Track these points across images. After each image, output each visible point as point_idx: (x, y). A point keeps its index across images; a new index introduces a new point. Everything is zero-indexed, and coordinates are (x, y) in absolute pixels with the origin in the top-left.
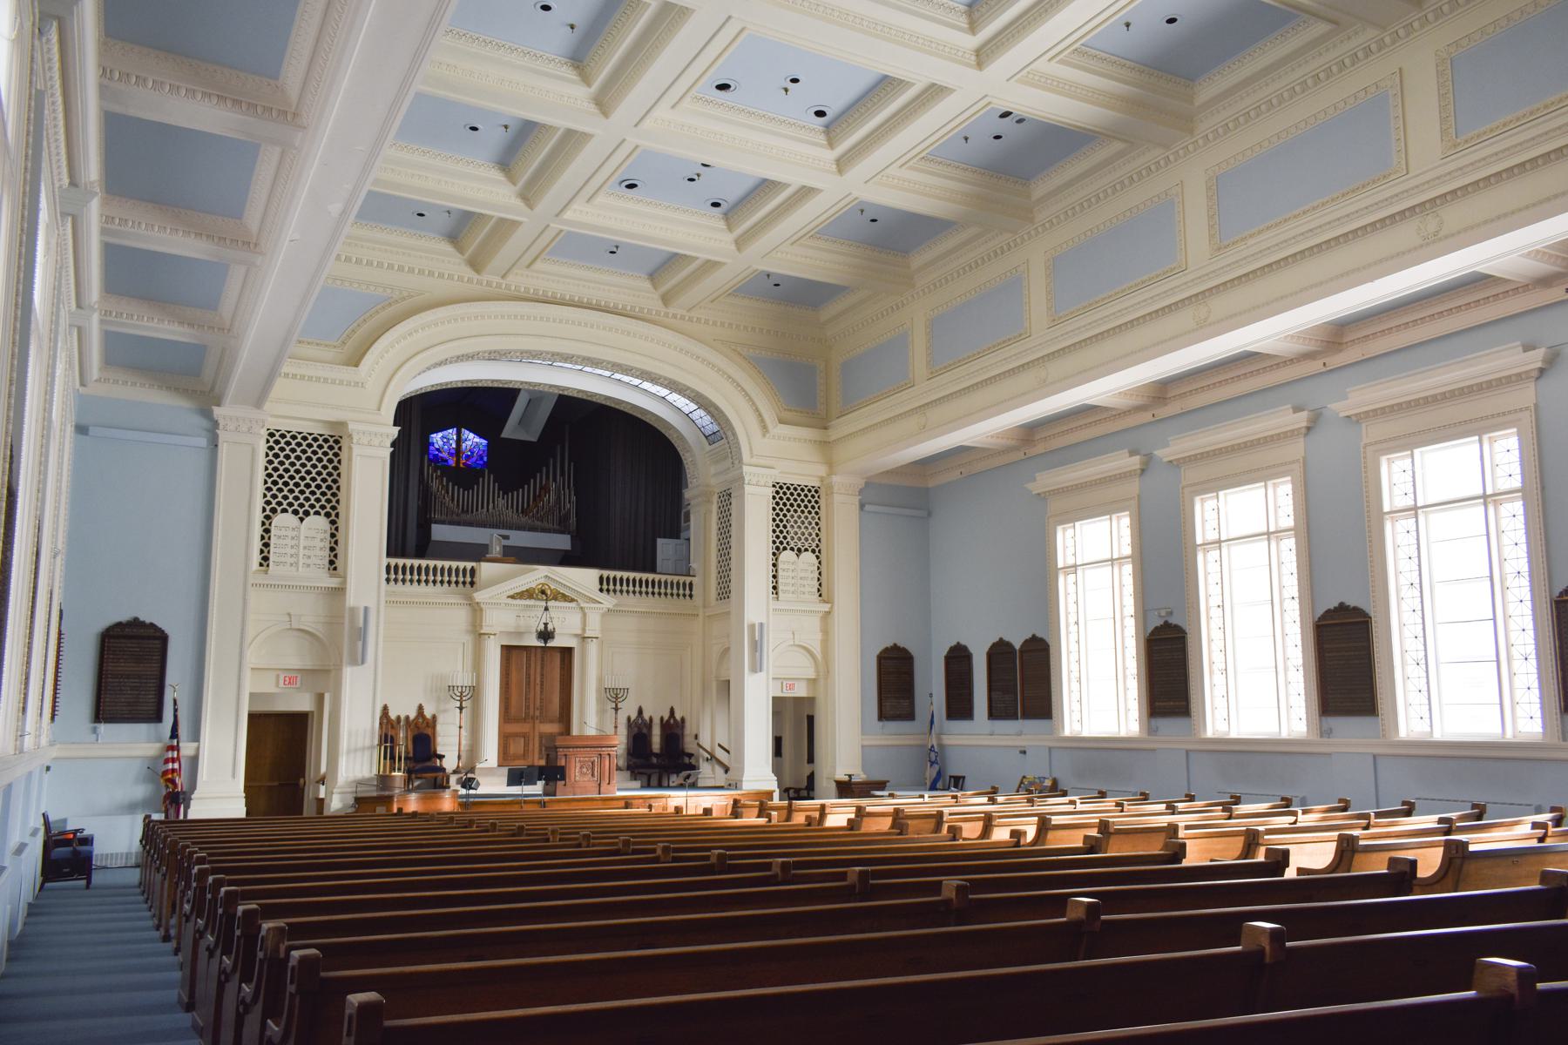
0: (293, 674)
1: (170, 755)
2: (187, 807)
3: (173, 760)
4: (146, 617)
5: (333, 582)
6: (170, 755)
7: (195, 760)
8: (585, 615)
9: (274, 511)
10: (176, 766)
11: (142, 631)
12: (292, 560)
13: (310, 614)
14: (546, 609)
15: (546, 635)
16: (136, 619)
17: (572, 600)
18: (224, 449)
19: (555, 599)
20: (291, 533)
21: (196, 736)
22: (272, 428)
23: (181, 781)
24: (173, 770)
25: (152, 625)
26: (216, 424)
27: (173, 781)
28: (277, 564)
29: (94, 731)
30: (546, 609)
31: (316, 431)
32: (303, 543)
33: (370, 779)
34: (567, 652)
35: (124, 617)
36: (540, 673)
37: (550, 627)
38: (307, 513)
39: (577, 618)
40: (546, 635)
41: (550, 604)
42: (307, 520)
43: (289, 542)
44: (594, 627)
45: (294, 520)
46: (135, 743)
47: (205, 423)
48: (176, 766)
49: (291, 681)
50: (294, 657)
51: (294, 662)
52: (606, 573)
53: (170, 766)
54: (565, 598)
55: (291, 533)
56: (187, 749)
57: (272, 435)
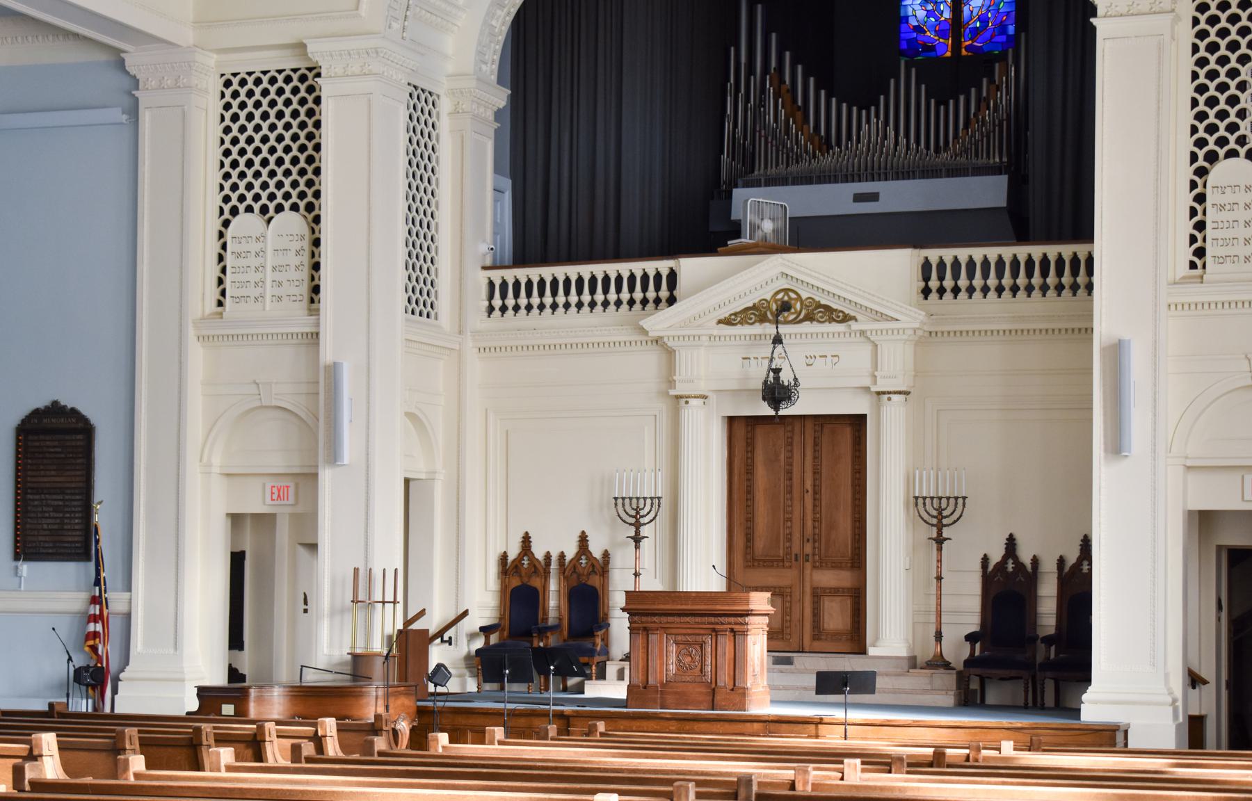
0: (282, 483)
1: (96, 610)
2: (115, 691)
3: (95, 618)
4: (68, 401)
5: (303, 324)
6: (96, 610)
7: (128, 616)
8: (670, 353)
9: (234, 211)
10: (99, 627)
11: (61, 422)
12: (256, 292)
13: (282, 376)
14: (777, 340)
15: (776, 392)
16: (55, 403)
17: (846, 318)
18: (146, 117)
19: (810, 318)
20: (254, 247)
21: (128, 587)
22: (228, 72)
23: (110, 650)
24: (95, 635)
25: (74, 412)
26: (135, 82)
27: (94, 649)
28: (237, 299)
29: (16, 571)
30: (777, 340)
31: (288, 65)
32: (270, 261)
33: (341, 664)
34: (857, 423)
35: (42, 402)
36: (796, 475)
37: (786, 377)
38: (280, 208)
39: (868, 348)
40: (776, 392)
41: (783, 329)
42: (278, 218)
43: (254, 262)
44: (896, 365)
45: (255, 219)
46: (56, 588)
47: (126, 83)
48: (99, 627)
49: (280, 494)
50: (274, 453)
51: (277, 462)
52: (934, 254)
53: (91, 627)
54: (832, 315)
55: (254, 247)
56: (116, 601)
57: (228, 84)
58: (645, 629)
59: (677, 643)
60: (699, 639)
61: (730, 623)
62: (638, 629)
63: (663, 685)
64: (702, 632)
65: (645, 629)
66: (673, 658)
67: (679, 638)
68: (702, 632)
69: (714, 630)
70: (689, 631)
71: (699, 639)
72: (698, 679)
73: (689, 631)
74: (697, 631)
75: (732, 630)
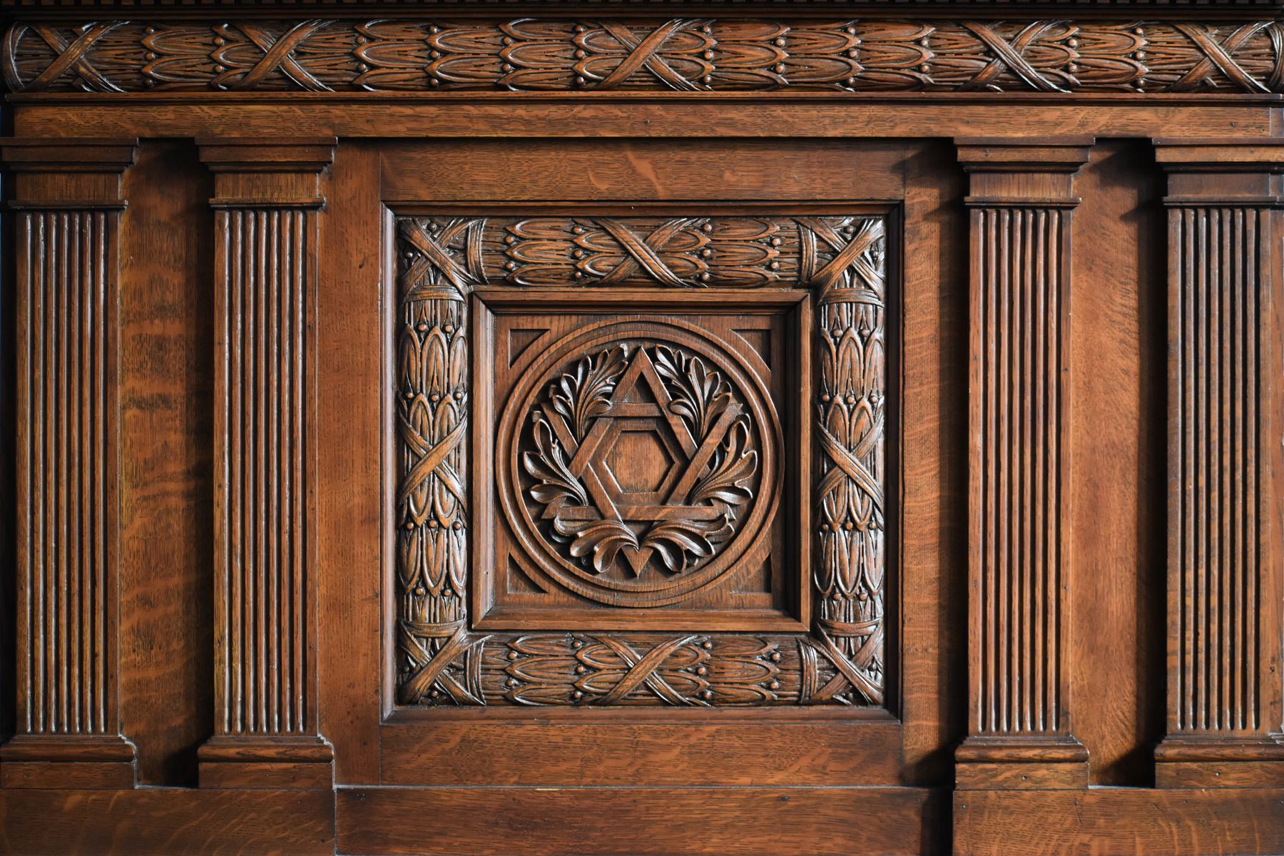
58: (184, 162)
59: (505, 296)
60: (763, 253)
61: (1101, 88)
62: (100, 158)
63: (367, 737)
64: (794, 178)
65: (184, 162)
66: (462, 463)
67: (546, 247)
68: (794, 178)
69: (939, 159)
70: (653, 176)
71: (763, 253)
72: (747, 673)
73: (653, 176)
74: (740, 176)
75: (1134, 160)
